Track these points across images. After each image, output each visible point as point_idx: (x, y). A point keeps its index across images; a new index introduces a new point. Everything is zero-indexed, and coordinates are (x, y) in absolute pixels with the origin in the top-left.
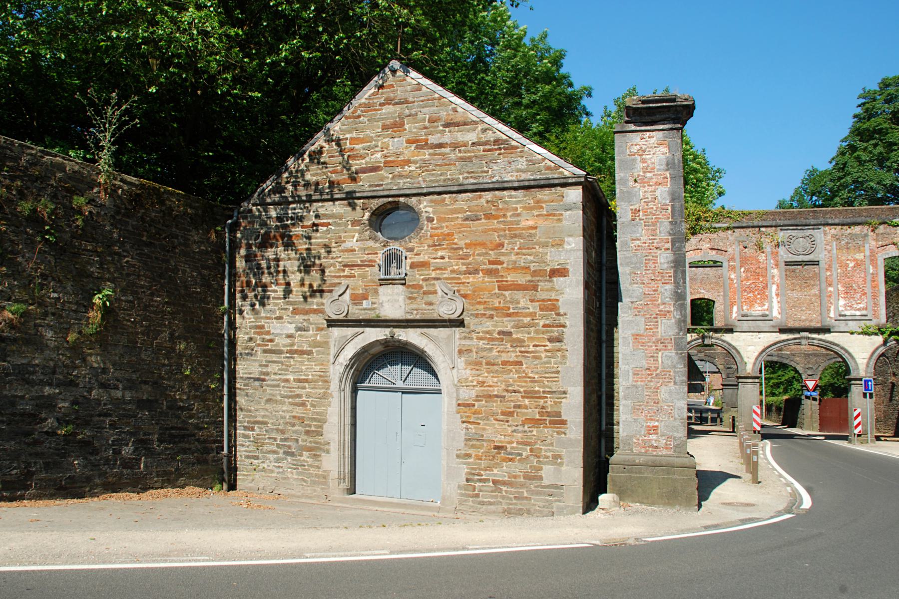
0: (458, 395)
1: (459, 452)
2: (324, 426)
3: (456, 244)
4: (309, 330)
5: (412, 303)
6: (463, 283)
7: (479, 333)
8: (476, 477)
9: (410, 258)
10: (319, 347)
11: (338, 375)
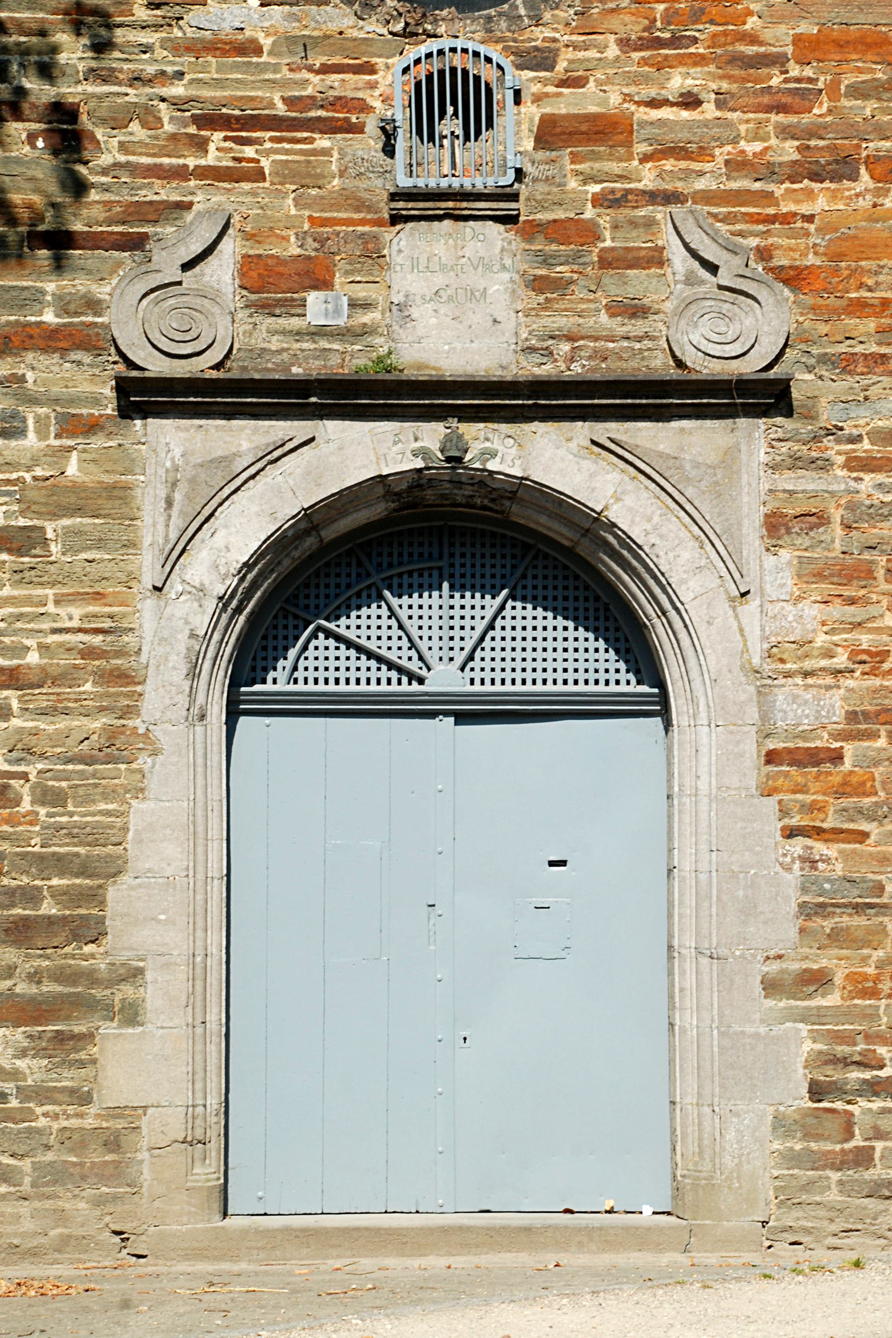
0: (765, 717)
1: (774, 967)
2: (111, 893)
3: (753, 39)
4: (21, 432)
5: (546, 306)
6: (787, 219)
7: (855, 439)
8: (856, 1075)
9: (538, 99)
10: (78, 511)
11: (182, 642)
